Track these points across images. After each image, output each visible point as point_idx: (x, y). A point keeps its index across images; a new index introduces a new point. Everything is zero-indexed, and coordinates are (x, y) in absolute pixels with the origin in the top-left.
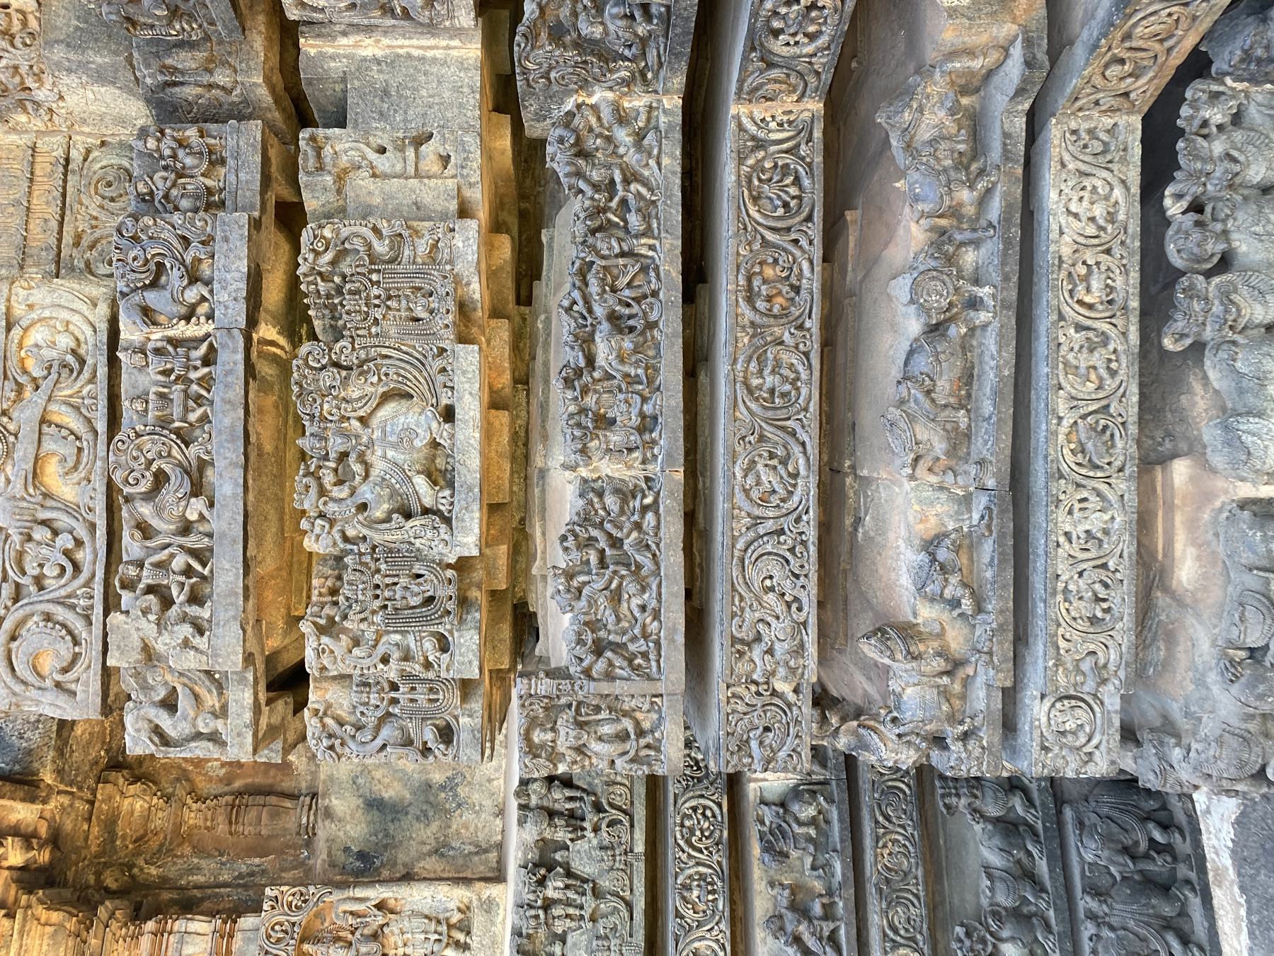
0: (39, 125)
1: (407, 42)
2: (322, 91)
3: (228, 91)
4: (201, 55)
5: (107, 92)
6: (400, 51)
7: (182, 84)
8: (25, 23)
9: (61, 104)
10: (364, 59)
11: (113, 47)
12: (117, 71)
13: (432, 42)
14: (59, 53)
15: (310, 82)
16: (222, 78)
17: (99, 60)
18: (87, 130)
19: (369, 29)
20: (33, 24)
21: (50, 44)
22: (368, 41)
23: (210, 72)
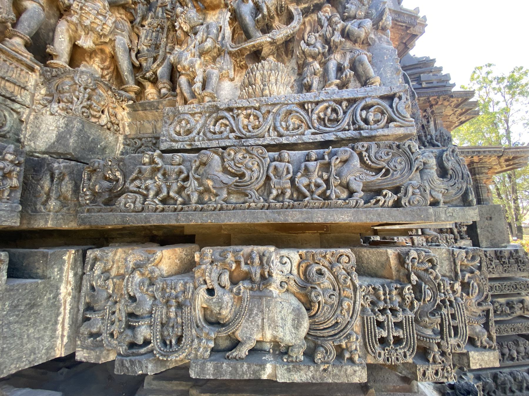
0: (38, 97)
1: (67, 311)
2: (38, 261)
3: (45, 203)
4: (69, 194)
5: (53, 137)
6: (62, 309)
7: (52, 180)
8: (94, 116)
9: (48, 113)
10: (58, 288)
11: (78, 149)
12: (64, 145)
13: (67, 326)
14: (77, 125)
15: (45, 255)
16: (53, 204)
17: (71, 141)
18: (32, 117)
19: (78, 287)
20: (93, 120)
21: (82, 122)
22: (70, 288)
23: (58, 198)
